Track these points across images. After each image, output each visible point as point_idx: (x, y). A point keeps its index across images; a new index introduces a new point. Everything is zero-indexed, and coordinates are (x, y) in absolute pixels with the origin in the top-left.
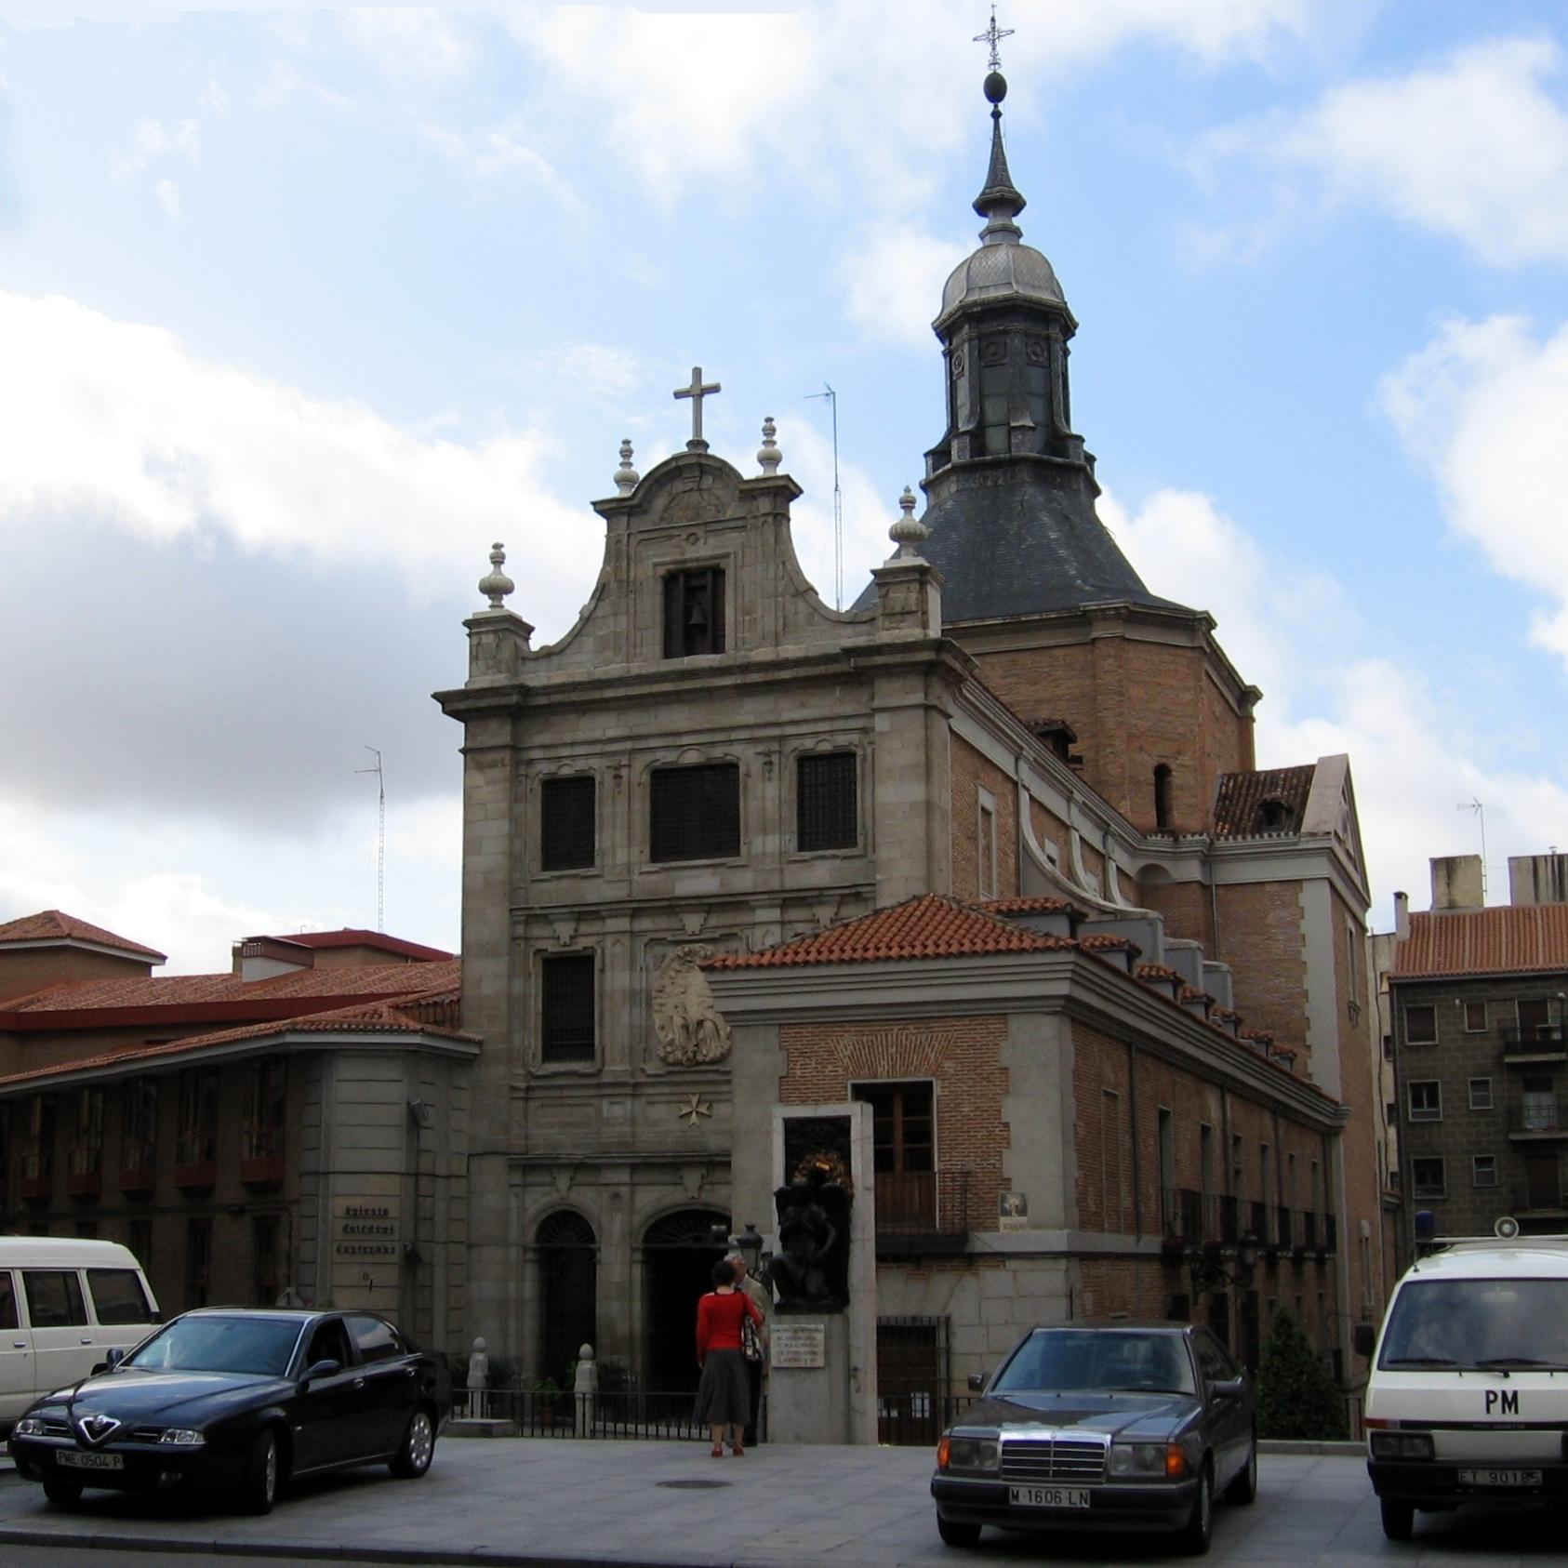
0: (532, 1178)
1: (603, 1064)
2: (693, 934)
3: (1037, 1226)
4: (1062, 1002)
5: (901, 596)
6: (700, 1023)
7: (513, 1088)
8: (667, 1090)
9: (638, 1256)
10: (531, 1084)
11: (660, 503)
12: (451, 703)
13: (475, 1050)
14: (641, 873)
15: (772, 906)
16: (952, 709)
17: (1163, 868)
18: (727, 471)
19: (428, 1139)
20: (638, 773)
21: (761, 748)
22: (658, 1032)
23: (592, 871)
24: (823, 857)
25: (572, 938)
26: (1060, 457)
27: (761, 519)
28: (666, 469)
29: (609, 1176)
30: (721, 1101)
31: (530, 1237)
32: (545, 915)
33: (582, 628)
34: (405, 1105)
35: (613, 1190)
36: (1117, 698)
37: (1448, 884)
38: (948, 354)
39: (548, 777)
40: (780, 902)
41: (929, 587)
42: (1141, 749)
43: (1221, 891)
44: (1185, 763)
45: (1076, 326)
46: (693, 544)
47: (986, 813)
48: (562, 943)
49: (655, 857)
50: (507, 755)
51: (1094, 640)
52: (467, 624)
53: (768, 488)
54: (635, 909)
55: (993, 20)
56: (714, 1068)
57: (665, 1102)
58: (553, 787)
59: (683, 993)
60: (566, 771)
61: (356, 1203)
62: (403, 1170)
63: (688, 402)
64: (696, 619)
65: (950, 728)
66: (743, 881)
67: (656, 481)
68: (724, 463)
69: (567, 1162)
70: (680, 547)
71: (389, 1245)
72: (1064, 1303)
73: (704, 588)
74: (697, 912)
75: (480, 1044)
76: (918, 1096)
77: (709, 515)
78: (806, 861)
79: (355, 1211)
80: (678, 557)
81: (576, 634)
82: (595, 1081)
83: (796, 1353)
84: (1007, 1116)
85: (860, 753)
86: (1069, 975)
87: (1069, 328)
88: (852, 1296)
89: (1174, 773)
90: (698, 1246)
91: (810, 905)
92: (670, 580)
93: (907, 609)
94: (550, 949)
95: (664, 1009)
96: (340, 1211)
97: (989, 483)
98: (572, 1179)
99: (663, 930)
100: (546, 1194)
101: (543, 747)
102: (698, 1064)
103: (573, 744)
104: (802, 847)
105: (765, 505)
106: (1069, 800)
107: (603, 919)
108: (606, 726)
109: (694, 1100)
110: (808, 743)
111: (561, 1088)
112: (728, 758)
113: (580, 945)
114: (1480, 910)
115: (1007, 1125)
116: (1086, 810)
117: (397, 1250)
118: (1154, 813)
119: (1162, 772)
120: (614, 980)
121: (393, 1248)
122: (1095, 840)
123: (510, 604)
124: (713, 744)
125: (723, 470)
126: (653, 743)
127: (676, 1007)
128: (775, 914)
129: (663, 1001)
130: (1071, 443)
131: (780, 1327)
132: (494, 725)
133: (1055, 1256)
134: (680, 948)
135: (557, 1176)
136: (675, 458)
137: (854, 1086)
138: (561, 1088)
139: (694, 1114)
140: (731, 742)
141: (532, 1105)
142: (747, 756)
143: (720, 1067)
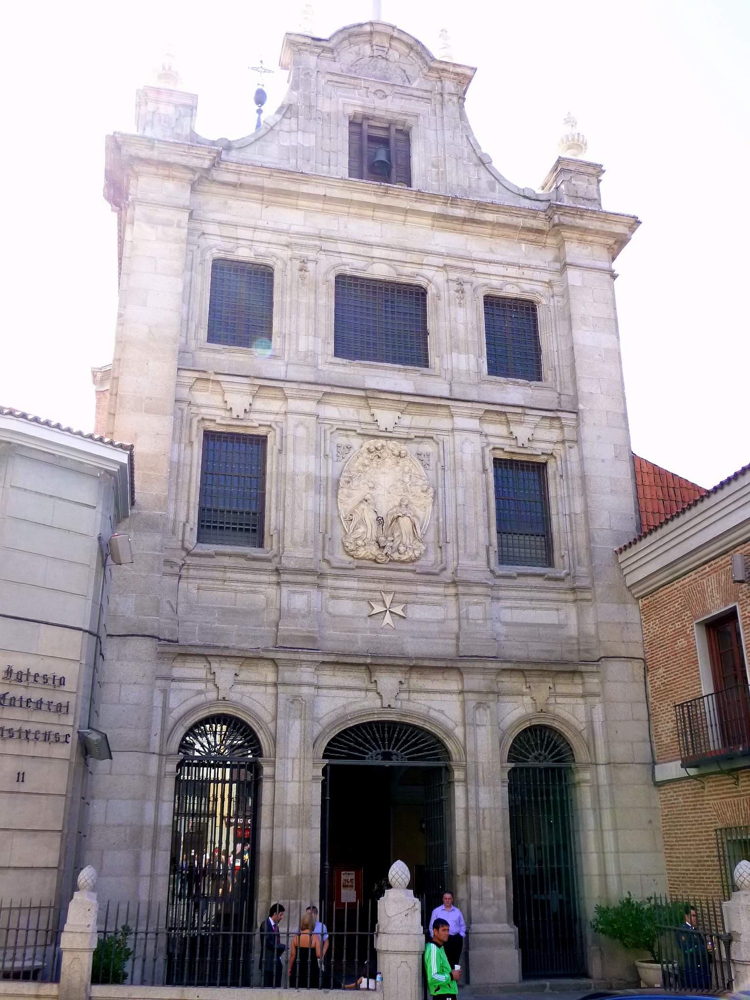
0: (180, 670)
7: (167, 562)
8: (354, 584)
9: (320, 772)
10: (188, 562)
11: (348, 56)
15: (471, 417)
18: (419, 49)
21: (454, 275)
24: (515, 383)
29: (287, 674)
30: (414, 603)
32: (218, 382)
34: (96, 538)
39: (222, 255)
40: (481, 413)
48: (235, 416)
53: (457, 74)
54: (325, 394)
56: (410, 567)
57: (353, 599)
60: (244, 254)
61: (20, 664)
62: (87, 627)
64: (382, 156)
66: (440, 388)
74: (389, 409)
80: (369, 104)
85: (544, 301)
90: (387, 763)
93: (589, 196)
95: (350, 501)
101: (220, 223)
103: (255, 228)
109: (388, 599)
110: (495, 282)
113: (255, 424)
126: (341, 247)
128: (474, 424)
132: (170, 186)
134: (372, 441)
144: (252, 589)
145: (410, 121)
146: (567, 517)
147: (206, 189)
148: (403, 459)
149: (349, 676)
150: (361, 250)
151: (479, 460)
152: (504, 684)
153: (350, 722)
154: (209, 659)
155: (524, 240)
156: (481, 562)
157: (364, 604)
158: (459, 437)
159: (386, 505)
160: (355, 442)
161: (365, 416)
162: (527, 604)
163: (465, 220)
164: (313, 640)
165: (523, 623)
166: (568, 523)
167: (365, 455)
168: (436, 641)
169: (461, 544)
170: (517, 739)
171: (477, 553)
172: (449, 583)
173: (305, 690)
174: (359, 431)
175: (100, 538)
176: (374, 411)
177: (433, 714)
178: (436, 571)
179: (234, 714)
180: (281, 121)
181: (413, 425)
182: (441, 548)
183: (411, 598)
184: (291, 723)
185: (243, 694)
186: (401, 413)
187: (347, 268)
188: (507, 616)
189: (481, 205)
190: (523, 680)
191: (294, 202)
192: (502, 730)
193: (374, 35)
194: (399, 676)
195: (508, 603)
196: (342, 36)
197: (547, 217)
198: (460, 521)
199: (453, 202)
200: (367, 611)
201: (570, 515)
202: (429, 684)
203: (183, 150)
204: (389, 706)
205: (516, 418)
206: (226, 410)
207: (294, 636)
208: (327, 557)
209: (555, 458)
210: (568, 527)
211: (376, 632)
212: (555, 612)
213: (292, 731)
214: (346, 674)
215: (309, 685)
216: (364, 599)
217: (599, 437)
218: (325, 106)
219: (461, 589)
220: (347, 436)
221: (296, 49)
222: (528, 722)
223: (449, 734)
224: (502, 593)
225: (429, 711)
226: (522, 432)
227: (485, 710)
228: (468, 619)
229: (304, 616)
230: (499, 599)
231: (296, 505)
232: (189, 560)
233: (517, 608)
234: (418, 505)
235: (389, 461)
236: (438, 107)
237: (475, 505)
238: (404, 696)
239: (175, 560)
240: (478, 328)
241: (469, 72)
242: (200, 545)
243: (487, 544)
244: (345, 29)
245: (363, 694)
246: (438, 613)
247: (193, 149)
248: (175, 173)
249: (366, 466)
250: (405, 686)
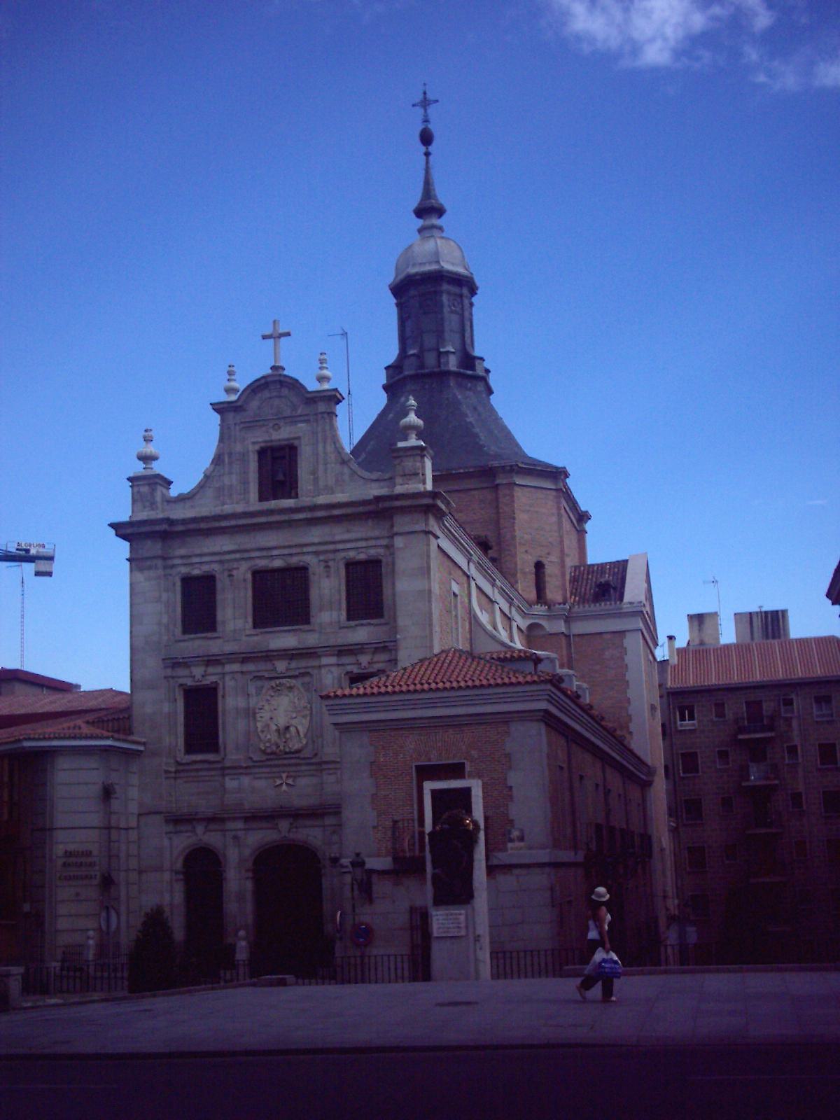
1: (225, 755)
2: (281, 673)
3: (530, 848)
4: (542, 714)
5: (410, 464)
6: (287, 728)
7: (167, 772)
9: (250, 874)
12: (121, 530)
13: (141, 748)
14: (247, 636)
15: (333, 655)
16: (439, 533)
17: (541, 625)
19: (116, 805)
20: (243, 572)
22: (260, 734)
23: (215, 635)
24: (362, 625)
25: (203, 676)
26: (470, 370)
27: (320, 416)
28: (258, 383)
29: (230, 825)
30: (299, 776)
31: (179, 865)
33: (206, 482)
35: (234, 833)
36: (512, 521)
37: (700, 630)
38: (400, 306)
40: (336, 652)
41: (426, 458)
42: (526, 551)
43: (577, 639)
44: (553, 560)
45: (477, 288)
46: (276, 430)
47: (455, 595)
49: (255, 626)
50: (160, 563)
51: (498, 485)
52: (130, 479)
53: (325, 396)
55: (425, 93)
56: (297, 755)
57: (266, 778)
58: (188, 582)
59: (275, 709)
60: (196, 572)
61: (71, 847)
62: (102, 825)
63: (271, 341)
64: (281, 477)
65: (439, 546)
66: (311, 640)
68: (297, 381)
69: (202, 817)
70: (267, 432)
71: (93, 873)
72: (548, 894)
73: (284, 457)
75: (144, 744)
76: (420, 769)
77: (288, 413)
78: (351, 627)
79: (71, 853)
80: (268, 439)
81: (201, 486)
82: (219, 766)
83: (448, 928)
84: (511, 782)
85: (384, 560)
86: (547, 697)
87: (473, 290)
88: (476, 894)
89: (546, 567)
91: (356, 655)
92: (262, 453)
94: (189, 684)
95: (263, 720)
96: (60, 853)
97: (427, 387)
99: (263, 671)
100: (189, 837)
101: (182, 557)
102: (286, 753)
103: (201, 555)
104: (349, 618)
105: (322, 407)
106: (493, 585)
107: (223, 664)
108: (224, 544)
109: (284, 775)
110: (352, 554)
111: (197, 770)
112: (301, 563)
113: (209, 680)
114: (719, 646)
115: (511, 788)
116: (503, 593)
117: (98, 877)
118: (535, 592)
119: (539, 566)
120: (230, 702)
121: (96, 875)
122: (506, 610)
123: (157, 468)
124: (291, 555)
125: (294, 385)
126: (253, 554)
127: (271, 718)
128: (333, 660)
129: (262, 715)
130: (477, 362)
131: (438, 913)
132: (149, 543)
133: (542, 865)
136: (264, 377)
137: (417, 767)
138: (197, 770)
140: (304, 553)
141: (179, 781)
142: (311, 560)
143: (301, 755)
145: (296, 443)
150: (265, 553)
151: (336, 681)
158: (323, 671)
161: (268, 666)
173: (239, 833)
174: (267, 676)
175: (103, 783)
176: (273, 662)
180: (214, 471)
183: (298, 774)
194: (291, 820)
202: (308, 822)
206: (191, 677)
208: (252, 755)
218: (238, 448)
219: (324, 766)
226: (364, 659)
232: (181, 768)
239: (170, 769)
241: (333, 393)
242: (187, 757)
244: (248, 386)
249: (272, 696)
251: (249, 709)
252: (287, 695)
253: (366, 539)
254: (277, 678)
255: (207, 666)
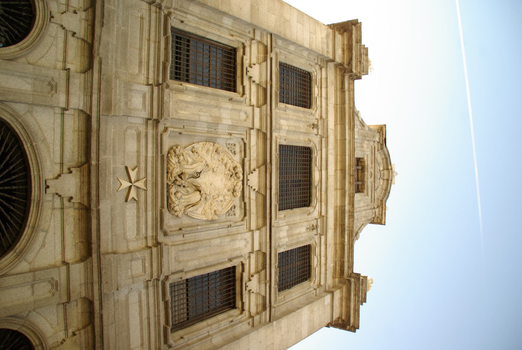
6: (198, 190)
15: (260, 244)
18: (387, 194)
30: (138, 209)
32: (265, 60)
57: (138, 152)
67: (386, 158)
74: (259, 182)
95: (204, 152)
98: (74, 34)
109: (141, 184)
135: (78, 16)
139: (131, 184)
143: (165, 210)
144: (143, 63)
146: (207, 334)
147: (338, 73)
148: (232, 194)
149: (74, 146)
152: (75, 308)
153: (29, 145)
154: (90, 10)
155: (336, 264)
156: (173, 268)
157: (134, 163)
159: (202, 181)
160: (237, 158)
162: (145, 316)
163: (343, 225)
164: (109, 107)
165: (129, 315)
166: (204, 336)
167: (232, 165)
168: (110, 232)
169: (186, 247)
170: (17, 334)
171: (180, 262)
172: (156, 239)
177: (41, 235)
178: (165, 227)
179: (35, 26)
181: (251, 200)
182: (180, 229)
183: (142, 206)
184: (29, 80)
185: (55, 38)
186: (257, 191)
187: (316, 154)
188: (134, 298)
189: (352, 232)
190: (80, 326)
191: (339, 123)
192: (28, 315)
193: (387, 171)
195: (144, 298)
196: (386, 153)
197: (350, 275)
198: (200, 243)
199: (351, 216)
200: (131, 163)
201: (209, 336)
203: (358, 58)
204: (48, 187)
205: (263, 277)
207: (111, 92)
209: (241, 313)
210: (201, 337)
211: (114, 173)
212: (139, 343)
213: (20, 80)
214: (76, 143)
215: (68, 102)
216: (138, 162)
217: (261, 342)
220: (241, 151)
221: (379, 131)
222: (37, 342)
223: (20, 255)
224: (151, 289)
225: (43, 231)
227: (50, 292)
228: (131, 261)
229: (126, 103)
230: (147, 287)
231: (202, 107)
233: (140, 306)
234: (205, 209)
235: (230, 184)
236: (370, 207)
237: (210, 255)
238: (57, 203)
240: (298, 243)
243: (185, 270)
245: (58, 160)
246: (131, 233)
247: (359, 63)
248: (346, 54)
250: (66, 203)
251: (216, 133)
252: (225, 185)
253: (326, 264)
254: (243, 174)
255: (258, 85)
